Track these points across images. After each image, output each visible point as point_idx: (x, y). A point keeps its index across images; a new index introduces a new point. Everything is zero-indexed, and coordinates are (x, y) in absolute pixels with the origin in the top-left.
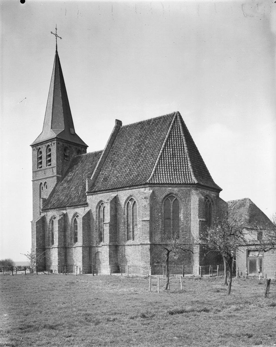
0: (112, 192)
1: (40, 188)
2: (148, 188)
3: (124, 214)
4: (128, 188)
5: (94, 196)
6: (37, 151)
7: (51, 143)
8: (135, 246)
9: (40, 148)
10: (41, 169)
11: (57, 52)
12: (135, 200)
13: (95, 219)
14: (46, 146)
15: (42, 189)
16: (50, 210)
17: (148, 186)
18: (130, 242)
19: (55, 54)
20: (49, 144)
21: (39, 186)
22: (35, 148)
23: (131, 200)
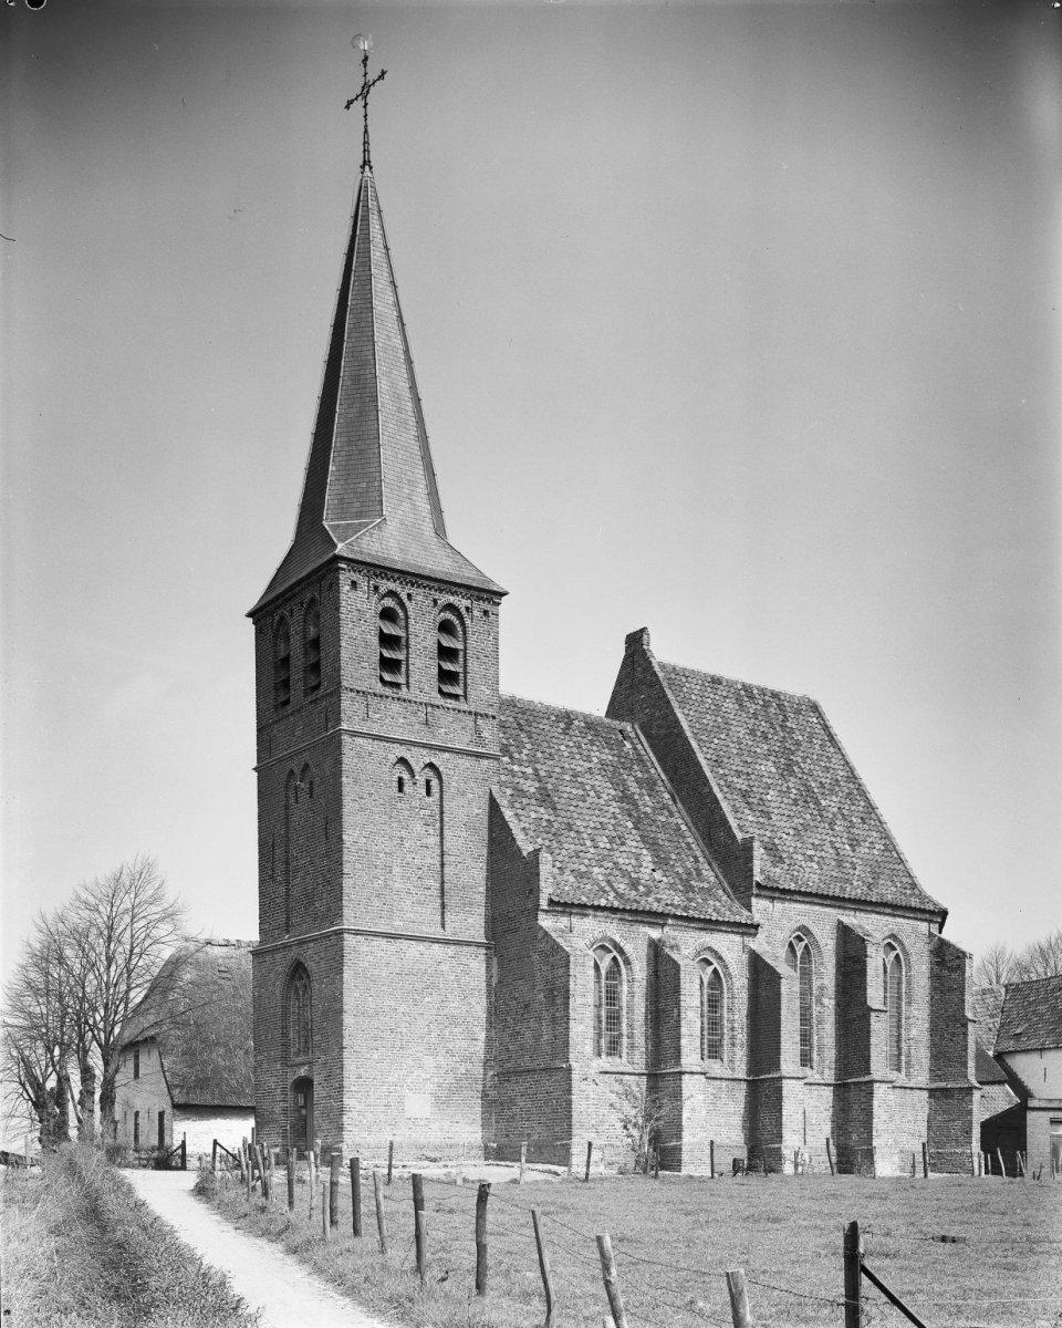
0: (839, 907)
4: (888, 911)
5: (779, 905)
16: (591, 912)
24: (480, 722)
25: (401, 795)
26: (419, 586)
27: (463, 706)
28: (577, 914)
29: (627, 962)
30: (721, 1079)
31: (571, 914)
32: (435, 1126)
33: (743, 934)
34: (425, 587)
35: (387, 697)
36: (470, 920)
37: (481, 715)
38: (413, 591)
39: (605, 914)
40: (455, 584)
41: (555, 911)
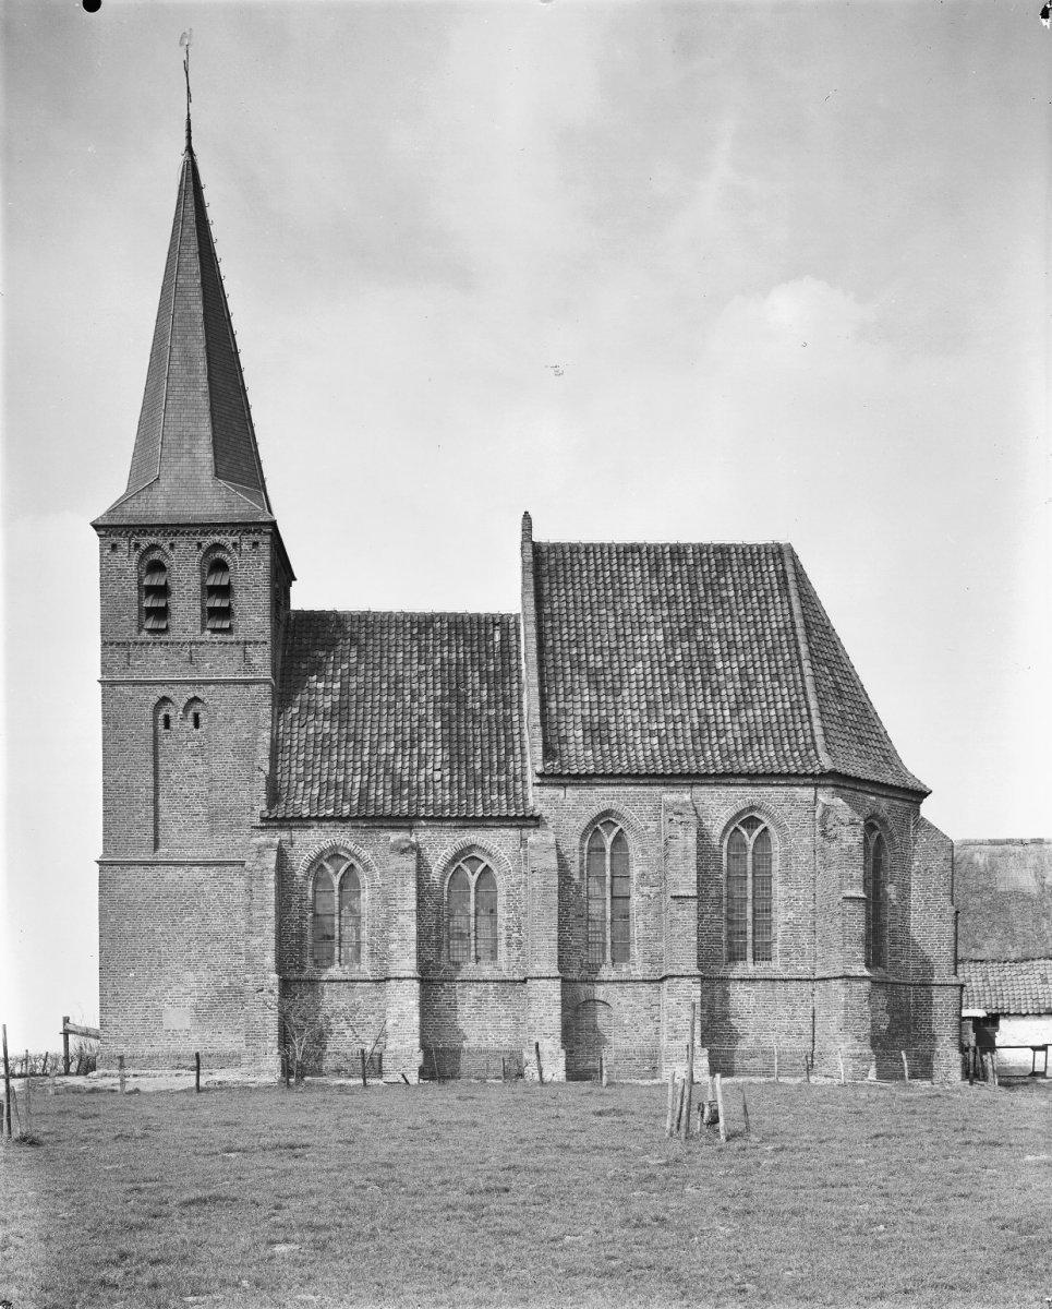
0: (664, 785)
1: (155, 720)
2: (832, 789)
3: (720, 871)
6: (136, 555)
7: (234, 539)
8: (769, 984)
9: (154, 547)
10: (164, 638)
11: (189, 149)
12: (767, 823)
13: (576, 877)
14: (199, 545)
15: (167, 726)
16: (314, 823)
17: (830, 782)
18: (748, 968)
19: (179, 159)
20: (227, 540)
21: (148, 711)
22: (114, 539)
23: (751, 823)
24: (249, 650)
25: (167, 731)
26: (182, 534)
27: (232, 638)
28: (296, 827)
29: (367, 868)
30: (486, 981)
31: (291, 828)
32: (195, 1037)
33: (521, 827)
34: (188, 534)
35: (149, 644)
36: (238, 841)
37: (250, 643)
38: (175, 540)
39: (332, 823)
40: (188, 525)
41: (269, 827)
